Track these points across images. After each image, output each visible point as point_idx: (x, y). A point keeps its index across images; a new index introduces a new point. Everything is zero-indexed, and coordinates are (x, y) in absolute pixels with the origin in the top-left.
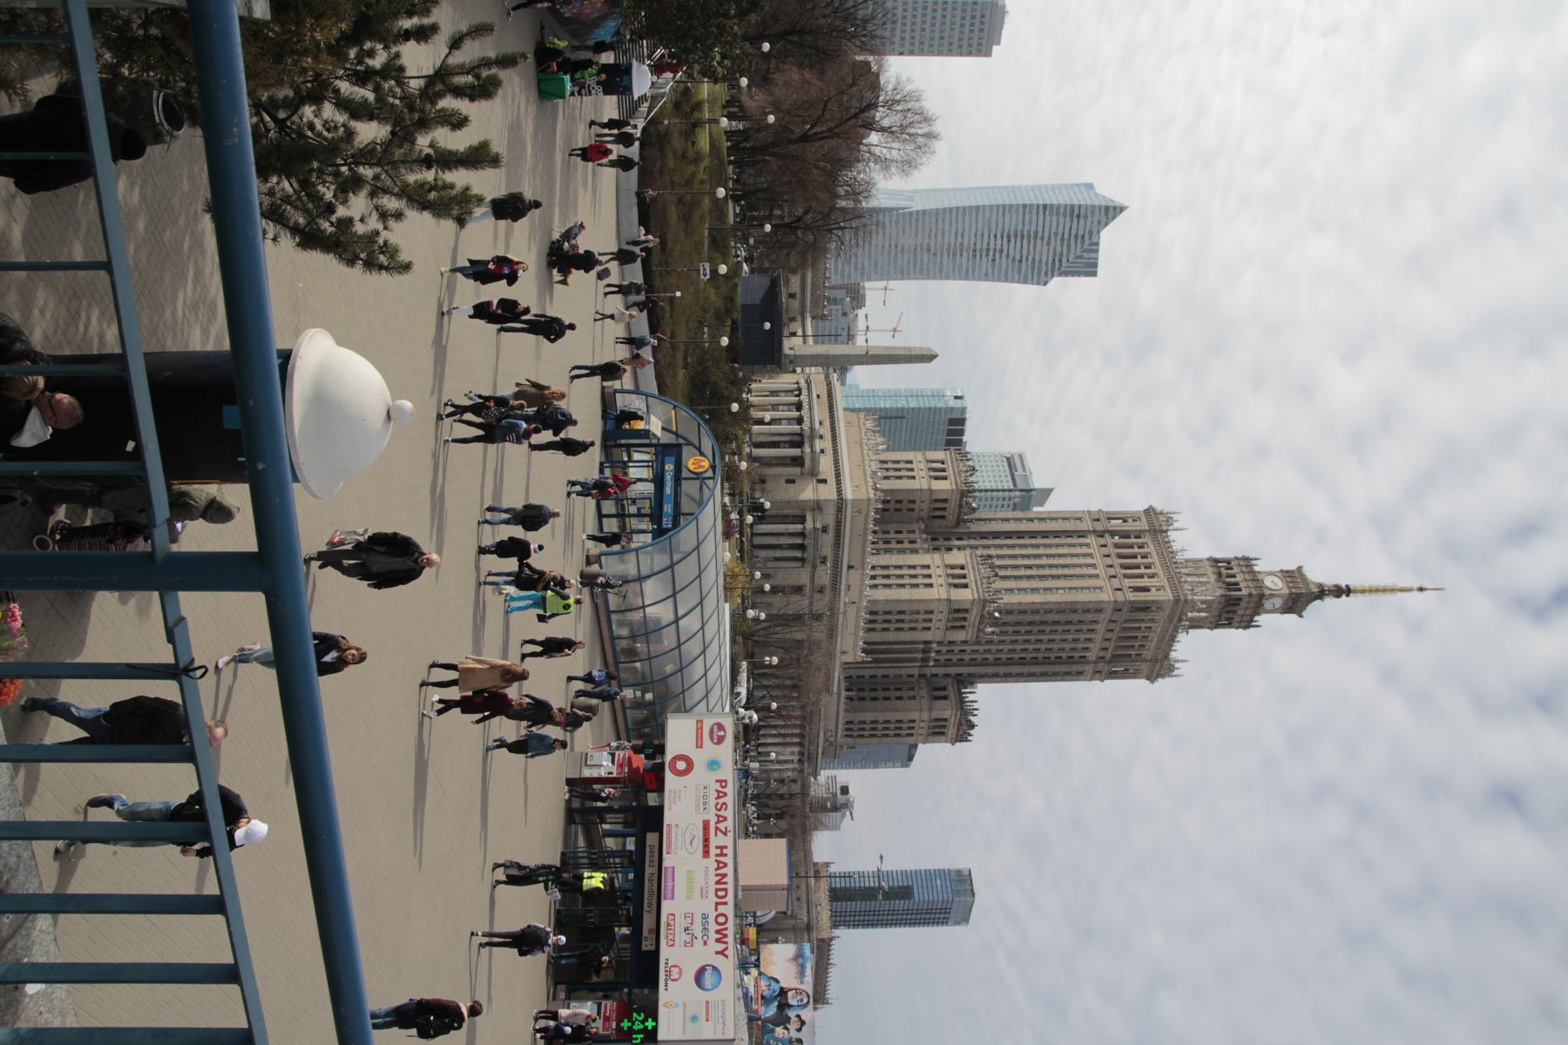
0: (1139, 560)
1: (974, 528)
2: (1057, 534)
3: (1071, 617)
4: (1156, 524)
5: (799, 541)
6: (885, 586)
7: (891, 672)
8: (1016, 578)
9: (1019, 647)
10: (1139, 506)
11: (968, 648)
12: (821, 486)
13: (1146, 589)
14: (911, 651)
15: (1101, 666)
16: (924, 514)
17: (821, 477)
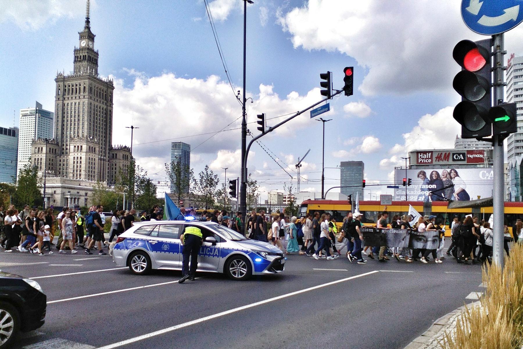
0: (74, 88)
1: (59, 140)
2: (63, 113)
3: (92, 113)
4: (60, 79)
5: (73, 199)
6: (80, 171)
7: (107, 170)
8: (78, 128)
9: (101, 130)
10: (54, 85)
11: (101, 146)
12: (56, 192)
13: (85, 87)
14: (101, 164)
15: (108, 104)
16: (54, 156)
17: (53, 192)
